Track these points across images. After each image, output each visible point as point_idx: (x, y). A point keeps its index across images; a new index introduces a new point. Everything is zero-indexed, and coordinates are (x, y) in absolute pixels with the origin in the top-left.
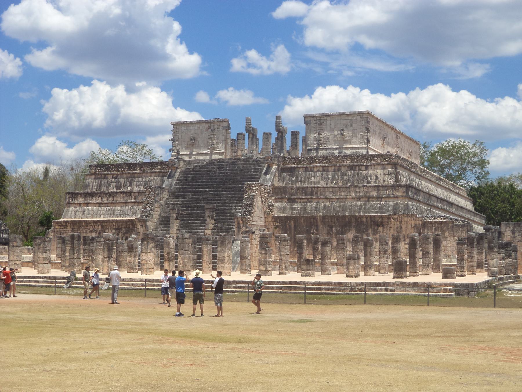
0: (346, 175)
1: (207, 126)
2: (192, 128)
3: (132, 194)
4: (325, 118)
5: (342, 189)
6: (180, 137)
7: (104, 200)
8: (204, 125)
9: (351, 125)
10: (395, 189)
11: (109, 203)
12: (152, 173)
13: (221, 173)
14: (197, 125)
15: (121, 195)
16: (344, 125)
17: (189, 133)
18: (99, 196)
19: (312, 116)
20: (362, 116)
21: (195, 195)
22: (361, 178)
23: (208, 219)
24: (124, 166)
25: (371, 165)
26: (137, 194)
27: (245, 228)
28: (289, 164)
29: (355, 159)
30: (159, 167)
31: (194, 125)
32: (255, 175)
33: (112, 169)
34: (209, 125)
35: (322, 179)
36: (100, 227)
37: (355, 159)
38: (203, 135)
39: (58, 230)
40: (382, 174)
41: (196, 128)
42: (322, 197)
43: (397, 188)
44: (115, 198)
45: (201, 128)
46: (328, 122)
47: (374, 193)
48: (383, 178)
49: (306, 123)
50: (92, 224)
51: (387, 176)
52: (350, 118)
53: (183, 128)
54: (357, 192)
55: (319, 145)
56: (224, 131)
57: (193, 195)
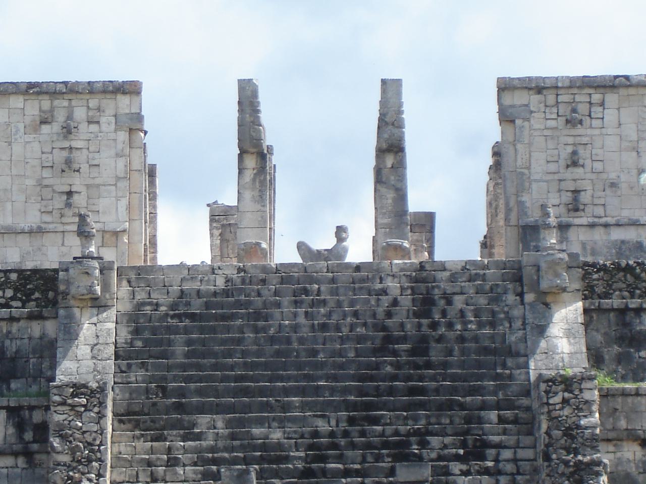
1: (33, 108)
4: (596, 98)
8: (17, 102)
13: (324, 327)
19: (537, 87)
21: (241, 423)
28: (607, 295)
32: (492, 338)
34: (46, 104)
38: (17, 149)
46: (610, 115)
49: (506, 117)
55: (575, 207)
56: (123, 136)
57: (229, 424)
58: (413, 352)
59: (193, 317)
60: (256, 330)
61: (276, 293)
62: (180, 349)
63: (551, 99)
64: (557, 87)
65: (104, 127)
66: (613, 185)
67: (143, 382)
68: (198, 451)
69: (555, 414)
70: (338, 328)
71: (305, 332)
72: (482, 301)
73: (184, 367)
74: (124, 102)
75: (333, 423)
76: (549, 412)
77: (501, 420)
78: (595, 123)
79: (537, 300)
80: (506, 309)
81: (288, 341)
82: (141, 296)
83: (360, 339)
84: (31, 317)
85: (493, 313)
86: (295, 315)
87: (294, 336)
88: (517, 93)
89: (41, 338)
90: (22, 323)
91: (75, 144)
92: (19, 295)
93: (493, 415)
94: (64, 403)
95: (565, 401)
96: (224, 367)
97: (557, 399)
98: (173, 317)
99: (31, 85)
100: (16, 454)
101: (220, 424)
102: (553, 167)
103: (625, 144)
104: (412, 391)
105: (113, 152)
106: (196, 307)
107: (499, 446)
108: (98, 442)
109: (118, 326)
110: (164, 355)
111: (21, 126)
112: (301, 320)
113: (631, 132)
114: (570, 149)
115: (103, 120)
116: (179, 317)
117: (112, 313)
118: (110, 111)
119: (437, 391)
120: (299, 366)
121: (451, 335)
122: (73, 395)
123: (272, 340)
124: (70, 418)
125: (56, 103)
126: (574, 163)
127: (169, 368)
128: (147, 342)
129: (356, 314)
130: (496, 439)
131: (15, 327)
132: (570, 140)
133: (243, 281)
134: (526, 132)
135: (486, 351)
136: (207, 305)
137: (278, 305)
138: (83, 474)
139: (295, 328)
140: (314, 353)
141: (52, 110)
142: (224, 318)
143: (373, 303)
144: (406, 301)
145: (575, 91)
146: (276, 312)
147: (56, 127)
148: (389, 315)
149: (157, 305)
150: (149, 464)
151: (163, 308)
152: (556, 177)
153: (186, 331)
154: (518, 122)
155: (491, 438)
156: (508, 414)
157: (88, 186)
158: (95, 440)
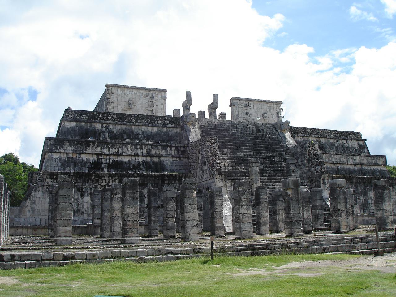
0: (334, 145)
1: (145, 93)
2: (128, 93)
3: (143, 147)
4: (250, 103)
5: (343, 156)
6: (115, 99)
7: (104, 150)
8: (141, 91)
9: (270, 111)
11: (113, 155)
12: (154, 127)
13: (241, 133)
14: (134, 90)
15: (129, 146)
16: (264, 110)
17: (126, 97)
18: (98, 146)
19: (240, 99)
20: (277, 105)
23: (293, 174)
24: (115, 116)
26: (149, 147)
30: (160, 122)
31: (131, 90)
33: (98, 117)
34: (147, 92)
36: (117, 181)
39: (51, 184)
41: (133, 93)
42: (330, 162)
43: (379, 158)
44: (120, 150)
45: (138, 94)
46: (252, 106)
47: (365, 161)
50: (106, 178)
53: (119, 91)
58: (262, 140)
59: (213, 129)
63: (242, 102)
64: (243, 100)
65: (159, 98)
66: (253, 119)
68: (227, 157)
69: (309, 151)
74: (163, 93)
75: (253, 153)
76: (308, 151)
79: (281, 131)
81: (235, 135)
82: (200, 124)
84: (174, 127)
88: (236, 100)
89: (176, 132)
90: (172, 129)
91: (153, 101)
92: (170, 123)
94: (209, 141)
95: (312, 149)
96: (224, 140)
97: (310, 148)
99: (145, 88)
100: (177, 157)
102: (243, 115)
103: (255, 112)
104: (265, 147)
105: (161, 103)
106: (213, 127)
111: (142, 96)
113: (256, 109)
114: (245, 112)
115: (159, 97)
116: (210, 129)
117: (196, 126)
118: (160, 95)
119: (270, 148)
122: (211, 140)
125: (149, 92)
126: (247, 114)
131: (170, 129)
132: (246, 110)
133: (220, 123)
135: (275, 140)
141: (148, 94)
142: (220, 130)
143: (248, 129)
144: (255, 130)
145: (246, 101)
147: (149, 97)
148: (253, 132)
149: (205, 126)
152: (243, 117)
154: (236, 106)
157: (156, 110)
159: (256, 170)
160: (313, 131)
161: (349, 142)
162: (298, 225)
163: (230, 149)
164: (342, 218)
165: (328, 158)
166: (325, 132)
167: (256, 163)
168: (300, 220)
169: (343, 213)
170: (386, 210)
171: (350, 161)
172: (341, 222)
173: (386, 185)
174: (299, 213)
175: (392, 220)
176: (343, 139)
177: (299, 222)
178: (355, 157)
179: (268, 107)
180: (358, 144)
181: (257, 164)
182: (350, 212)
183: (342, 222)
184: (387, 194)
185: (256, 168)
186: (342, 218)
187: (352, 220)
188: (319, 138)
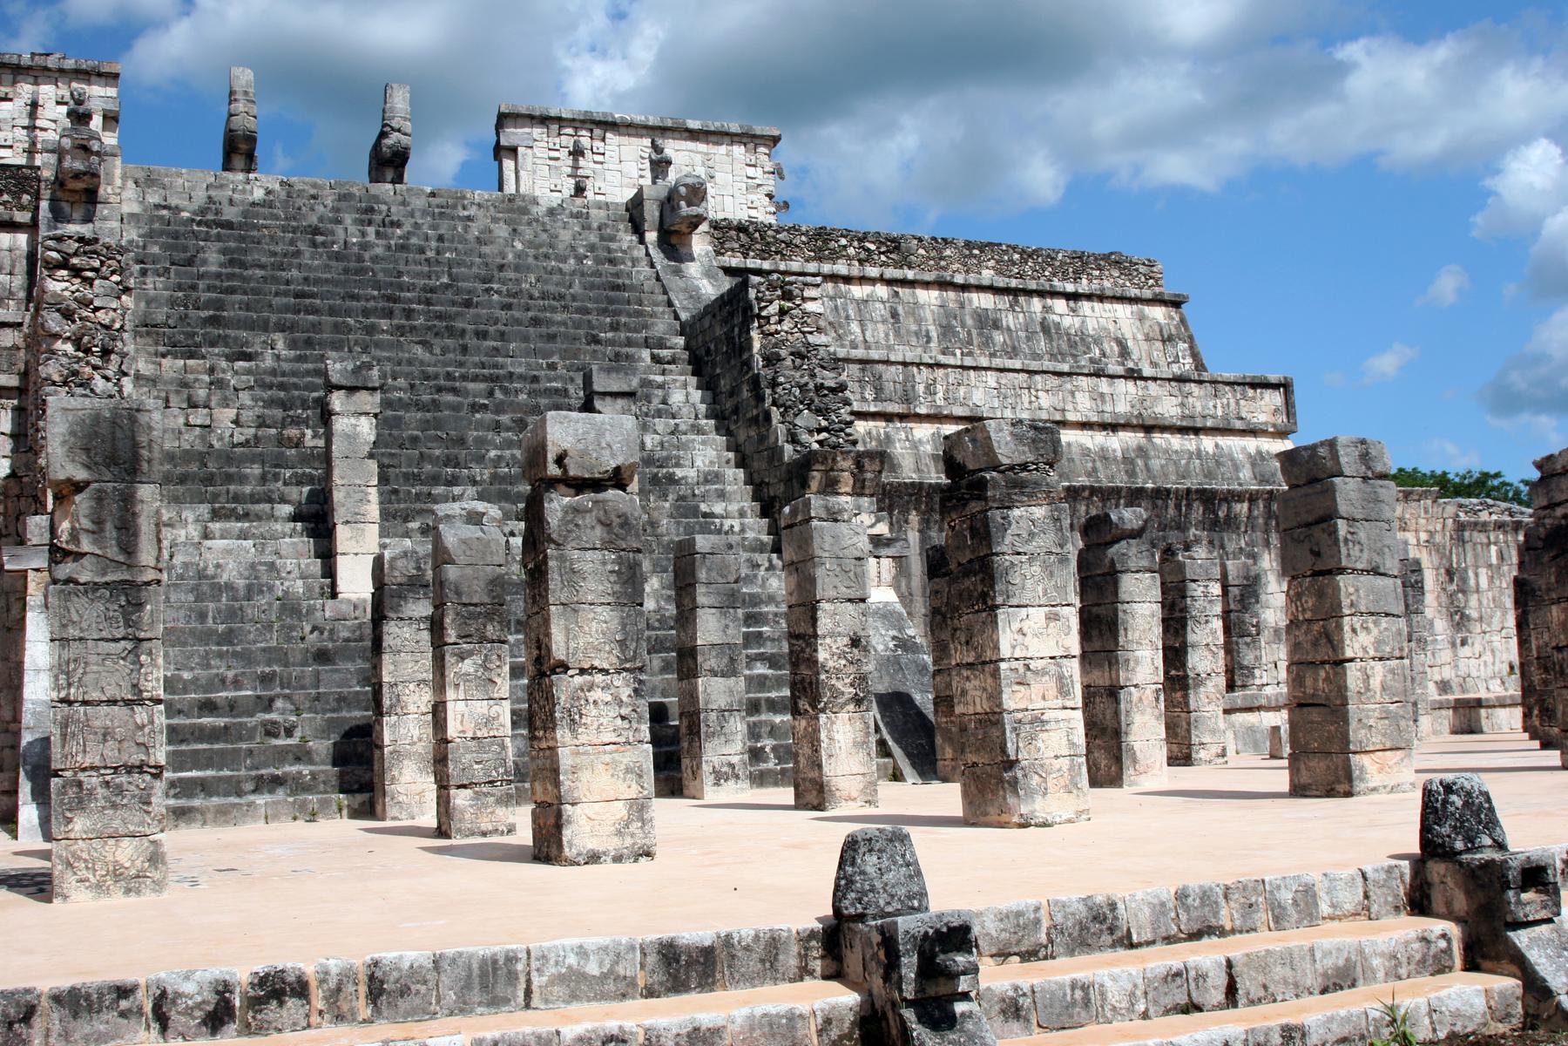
0: (996, 325)
5: (1038, 378)
10: (1244, 397)
13: (403, 248)
21: (309, 343)
22: (1064, 346)
25: (1089, 297)
27: (867, 519)
29: (1014, 264)
35: (897, 333)
37: (1014, 264)
40: (1140, 337)
43: (1250, 392)
47: (1168, 407)
48: (1150, 355)
51: (1159, 345)
52: (702, 147)
54: (1102, 395)
57: (292, 345)
59: (228, 225)
60: (314, 244)
61: (336, 210)
62: (213, 259)
67: (166, 289)
70: (422, 251)
71: (379, 251)
72: (593, 238)
73: (218, 276)
75: (438, 351)
77: (656, 359)
78: (599, 158)
80: (625, 247)
81: (360, 259)
82: (154, 198)
83: (450, 264)
85: (609, 251)
86: (363, 234)
87: (367, 256)
93: (646, 354)
95: (783, 312)
98: (199, 224)
101: (280, 345)
106: (230, 214)
107: (661, 386)
108: (117, 326)
109: (125, 226)
110: (190, 262)
112: (371, 237)
120: (377, 285)
121: (566, 267)
123: (338, 257)
124: (73, 288)
127: (201, 276)
128: (165, 247)
129: (441, 239)
130: (659, 379)
134: (529, 160)
135: (617, 288)
136: (245, 214)
137: (339, 222)
138: (95, 368)
139: (365, 246)
140: (400, 274)
146: (339, 230)
149: (177, 210)
150: (184, 384)
151: (185, 215)
153: (219, 238)
155: (652, 377)
156: (665, 353)
158: (113, 321)
159: (351, 437)
160: (873, 247)
161: (1085, 306)
162: (114, 806)
163: (281, 328)
164: (583, 739)
165: (947, 391)
166: (948, 252)
167: (352, 389)
168: (136, 758)
169: (597, 694)
170: (1019, 665)
171: (1080, 407)
172: (575, 770)
173: (1024, 467)
174: (128, 703)
175: (1072, 744)
176: (1054, 294)
177: (123, 779)
178: (1110, 385)
179: (698, 159)
180: (1142, 318)
181: (363, 396)
182: (839, 685)
183: (585, 776)
184: (1032, 535)
185: (353, 420)
186: (583, 739)
187: (855, 744)
188: (907, 291)
